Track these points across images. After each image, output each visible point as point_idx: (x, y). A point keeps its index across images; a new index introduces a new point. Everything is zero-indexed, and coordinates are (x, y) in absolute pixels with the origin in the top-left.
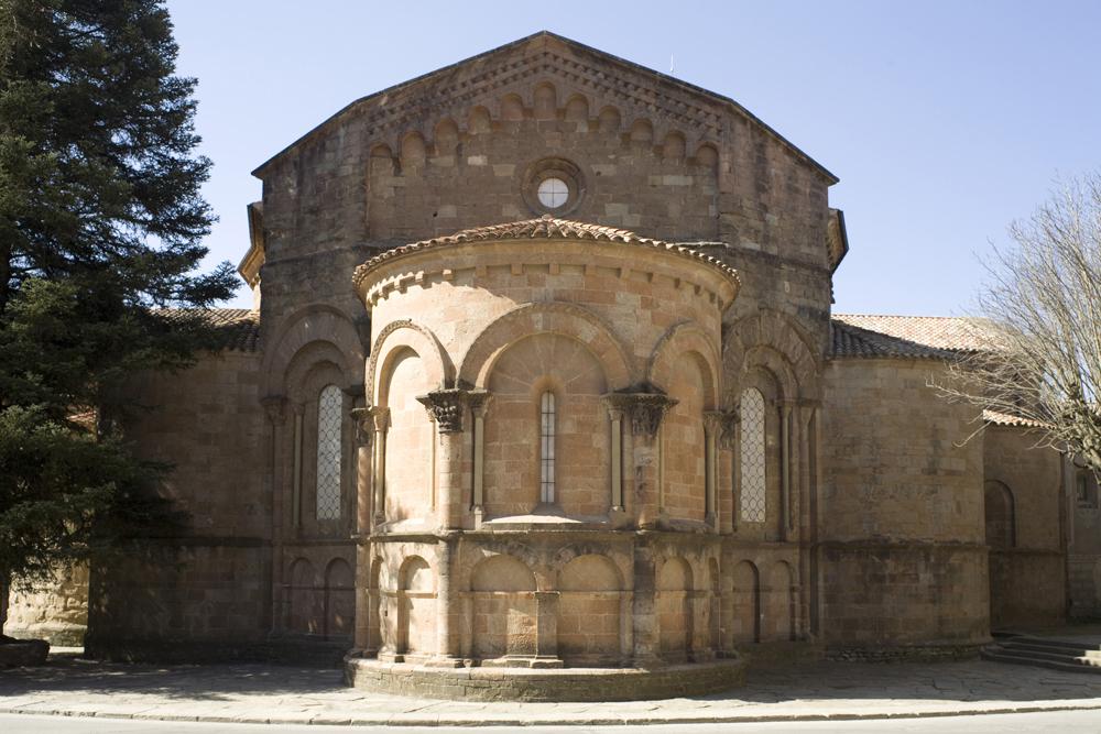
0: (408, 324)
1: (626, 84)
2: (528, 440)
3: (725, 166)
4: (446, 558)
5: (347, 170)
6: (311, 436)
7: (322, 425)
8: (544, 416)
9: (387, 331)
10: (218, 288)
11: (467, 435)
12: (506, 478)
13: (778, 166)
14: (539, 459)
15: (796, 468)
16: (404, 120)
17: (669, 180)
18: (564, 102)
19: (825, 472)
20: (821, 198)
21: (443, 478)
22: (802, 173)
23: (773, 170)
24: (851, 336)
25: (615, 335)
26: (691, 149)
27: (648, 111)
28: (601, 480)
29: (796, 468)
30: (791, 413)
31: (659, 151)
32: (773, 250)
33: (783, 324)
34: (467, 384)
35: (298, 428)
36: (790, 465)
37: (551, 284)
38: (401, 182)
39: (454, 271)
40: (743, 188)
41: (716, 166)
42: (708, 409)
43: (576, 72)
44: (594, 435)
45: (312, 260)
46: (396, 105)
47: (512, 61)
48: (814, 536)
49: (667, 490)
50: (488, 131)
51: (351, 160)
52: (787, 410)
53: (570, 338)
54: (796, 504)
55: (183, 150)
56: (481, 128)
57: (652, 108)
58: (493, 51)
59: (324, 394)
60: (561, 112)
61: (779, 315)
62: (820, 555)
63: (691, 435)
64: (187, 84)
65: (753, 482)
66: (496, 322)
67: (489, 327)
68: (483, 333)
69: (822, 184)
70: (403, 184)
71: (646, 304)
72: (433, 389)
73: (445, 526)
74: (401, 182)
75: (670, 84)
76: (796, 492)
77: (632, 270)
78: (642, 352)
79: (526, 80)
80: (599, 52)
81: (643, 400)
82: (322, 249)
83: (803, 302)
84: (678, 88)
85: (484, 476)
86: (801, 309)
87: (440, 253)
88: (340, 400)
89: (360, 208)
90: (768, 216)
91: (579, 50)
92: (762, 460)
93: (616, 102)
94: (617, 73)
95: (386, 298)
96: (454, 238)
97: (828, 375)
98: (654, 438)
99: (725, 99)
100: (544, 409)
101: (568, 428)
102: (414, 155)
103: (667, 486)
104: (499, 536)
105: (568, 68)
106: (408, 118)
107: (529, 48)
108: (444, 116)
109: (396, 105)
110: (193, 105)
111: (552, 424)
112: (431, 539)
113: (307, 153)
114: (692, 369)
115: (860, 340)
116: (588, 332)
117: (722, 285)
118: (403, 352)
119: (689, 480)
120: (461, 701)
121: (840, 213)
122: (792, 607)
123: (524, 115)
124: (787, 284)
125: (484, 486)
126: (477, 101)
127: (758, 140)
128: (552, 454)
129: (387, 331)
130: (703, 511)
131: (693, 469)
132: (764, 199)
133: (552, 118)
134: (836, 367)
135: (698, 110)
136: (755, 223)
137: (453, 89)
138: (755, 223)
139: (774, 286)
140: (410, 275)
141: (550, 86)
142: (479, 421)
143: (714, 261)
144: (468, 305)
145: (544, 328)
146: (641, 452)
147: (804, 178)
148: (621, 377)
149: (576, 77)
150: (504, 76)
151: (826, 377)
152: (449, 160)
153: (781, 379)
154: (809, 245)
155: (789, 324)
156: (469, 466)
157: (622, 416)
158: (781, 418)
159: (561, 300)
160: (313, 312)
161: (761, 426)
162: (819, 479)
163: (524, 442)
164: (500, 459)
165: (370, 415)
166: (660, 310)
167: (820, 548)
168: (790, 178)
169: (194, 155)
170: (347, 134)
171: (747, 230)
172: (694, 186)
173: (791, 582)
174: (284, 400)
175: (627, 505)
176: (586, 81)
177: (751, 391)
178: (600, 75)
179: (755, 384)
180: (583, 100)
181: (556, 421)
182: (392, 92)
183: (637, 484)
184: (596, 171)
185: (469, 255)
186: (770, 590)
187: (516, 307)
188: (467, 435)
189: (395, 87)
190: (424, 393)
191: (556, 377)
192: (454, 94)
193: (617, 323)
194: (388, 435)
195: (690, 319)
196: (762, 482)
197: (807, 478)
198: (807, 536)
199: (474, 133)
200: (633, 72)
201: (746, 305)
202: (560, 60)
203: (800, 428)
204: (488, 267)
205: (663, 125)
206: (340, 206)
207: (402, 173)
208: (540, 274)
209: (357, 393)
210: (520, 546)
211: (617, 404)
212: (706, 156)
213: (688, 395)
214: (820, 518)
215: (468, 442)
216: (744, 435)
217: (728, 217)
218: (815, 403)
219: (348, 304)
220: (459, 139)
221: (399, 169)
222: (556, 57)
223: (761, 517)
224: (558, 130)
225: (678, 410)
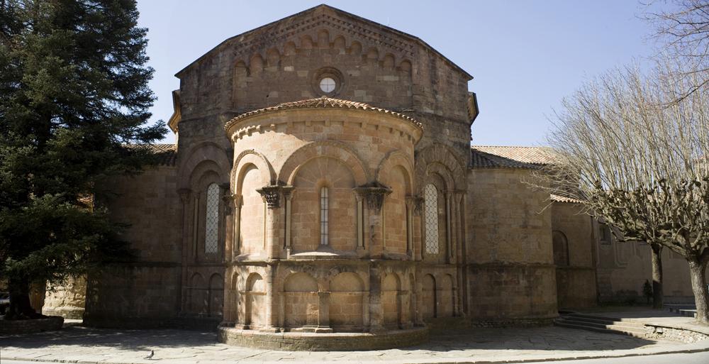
0: (252, 152)
1: (364, 31)
2: (314, 212)
3: (415, 71)
4: (271, 274)
5: (223, 73)
6: (203, 209)
7: (209, 204)
8: (322, 200)
9: (242, 155)
10: (157, 133)
11: (282, 210)
12: (302, 232)
13: (442, 71)
14: (320, 222)
15: (454, 225)
16: (252, 48)
17: (386, 78)
18: (333, 39)
19: (469, 227)
20: (465, 87)
21: (270, 232)
22: (454, 74)
23: (440, 73)
24: (482, 157)
25: (359, 157)
26: (398, 62)
27: (376, 44)
28: (352, 233)
29: (454, 225)
30: (451, 197)
31: (381, 64)
32: (440, 113)
33: (446, 151)
34: (282, 183)
35: (196, 206)
36: (451, 224)
37: (326, 131)
38: (250, 79)
39: (276, 125)
40: (424, 82)
41: (411, 71)
42: (408, 195)
43: (339, 24)
44: (348, 209)
45: (204, 119)
46: (248, 41)
47: (307, 19)
48: (464, 262)
49: (387, 238)
50: (295, 54)
51: (225, 69)
52: (449, 195)
53: (336, 159)
54: (455, 244)
55: (140, 64)
56: (291, 53)
57: (378, 42)
58: (297, 14)
59: (210, 187)
60: (332, 44)
61: (444, 147)
62: (468, 271)
63: (399, 209)
64: (143, 31)
65: (432, 232)
66: (297, 151)
67: (294, 153)
68: (291, 156)
69: (464, 80)
70: (250, 81)
71: (375, 141)
72: (265, 185)
74: (250, 79)
75: (387, 30)
76: (454, 238)
77: (368, 124)
78: (373, 166)
79: (314, 28)
80: (350, 14)
81: (374, 191)
82: (210, 114)
83: (456, 140)
84: (391, 32)
85: (291, 230)
86: (455, 143)
87: (269, 115)
88: (218, 191)
89: (229, 93)
90: (437, 96)
91: (341, 13)
92: (436, 221)
93: (359, 39)
94: (360, 25)
95: (241, 138)
96: (276, 108)
97: (470, 177)
98: (380, 210)
99: (414, 37)
100: (323, 195)
101: (335, 206)
102: (257, 66)
103: (387, 235)
104: (299, 262)
105: (335, 22)
106: (254, 47)
107: (315, 12)
108: (272, 47)
109: (248, 41)
110: (146, 42)
111: (327, 203)
112: (263, 264)
113: (203, 65)
114: (400, 175)
115: (486, 159)
116: (345, 155)
117: (415, 131)
118: (250, 166)
119: (398, 232)
121: (474, 94)
122: (454, 298)
123: (313, 45)
124: (448, 131)
125: (291, 236)
126: (289, 39)
127: (432, 58)
128: (326, 220)
129: (242, 155)
130: (406, 249)
131: (401, 227)
132: (435, 87)
133: (327, 47)
134: (474, 173)
135: (401, 43)
136: (431, 100)
137: (277, 33)
138: (431, 100)
139: (441, 132)
140: (254, 126)
141: (327, 32)
142: (289, 202)
143: (410, 119)
144: (284, 142)
145: (322, 154)
146: (373, 218)
147: (455, 78)
148: (362, 179)
149: (339, 27)
150: (303, 26)
151: (469, 178)
152: (274, 69)
153: (446, 180)
154: (459, 111)
155: (449, 151)
156: (283, 226)
157: (363, 200)
158: (446, 200)
159: (331, 139)
160: (205, 145)
161: (436, 203)
162: (466, 231)
163: (312, 213)
164: (299, 222)
165: (233, 199)
166: (382, 144)
167: (468, 267)
168: (448, 77)
169: (145, 66)
170: (223, 55)
171: (427, 103)
172: (400, 81)
173: (453, 285)
174: (189, 191)
175: (366, 245)
176: (344, 29)
177: (430, 185)
178: (352, 26)
179: (433, 182)
180: (342, 38)
181: (329, 202)
182: (246, 35)
183: (371, 235)
184: (349, 74)
185: (283, 117)
186: (441, 289)
187: (307, 143)
188: (282, 210)
189: (247, 32)
190: (260, 187)
191: (328, 179)
192: (277, 36)
193: (360, 151)
194: (242, 210)
195: (398, 148)
196: (437, 233)
197: (460, 230)
198: (461, 262)
199: (288, 55)
200: (368, 25)
201: (427, 142)
202: (331, 18)
203: (456, 205)
204: (294, 123)
205: (383, 51)
206: (219, 92)
207: (252, 75)
208: (320, 126)
209: (226, 187)
210: (310, 268)
211: (360, 194)
212: (406, 66)
213: (398, 190)
214: (467, 251)
215: (283, 213)
216: (427, 208)
217: (417, 96)
218: (464, 192)
219: (222, 142)
220: (280, 58)
221: (249, 74)
222: (329, 17)
223: (437, 251)
224: (330, 53)
225: (392, 196)
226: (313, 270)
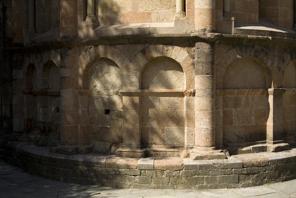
4: (210, 59)
73: (208, 29)
104: (251, 40)
120: (234, 188)
210: (263, 50)
226: (266, 53)
